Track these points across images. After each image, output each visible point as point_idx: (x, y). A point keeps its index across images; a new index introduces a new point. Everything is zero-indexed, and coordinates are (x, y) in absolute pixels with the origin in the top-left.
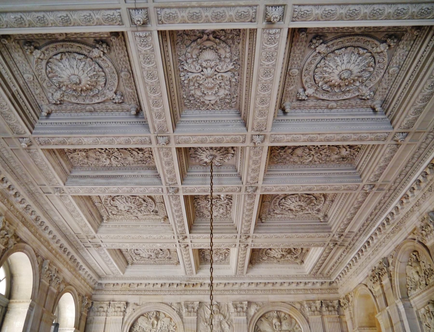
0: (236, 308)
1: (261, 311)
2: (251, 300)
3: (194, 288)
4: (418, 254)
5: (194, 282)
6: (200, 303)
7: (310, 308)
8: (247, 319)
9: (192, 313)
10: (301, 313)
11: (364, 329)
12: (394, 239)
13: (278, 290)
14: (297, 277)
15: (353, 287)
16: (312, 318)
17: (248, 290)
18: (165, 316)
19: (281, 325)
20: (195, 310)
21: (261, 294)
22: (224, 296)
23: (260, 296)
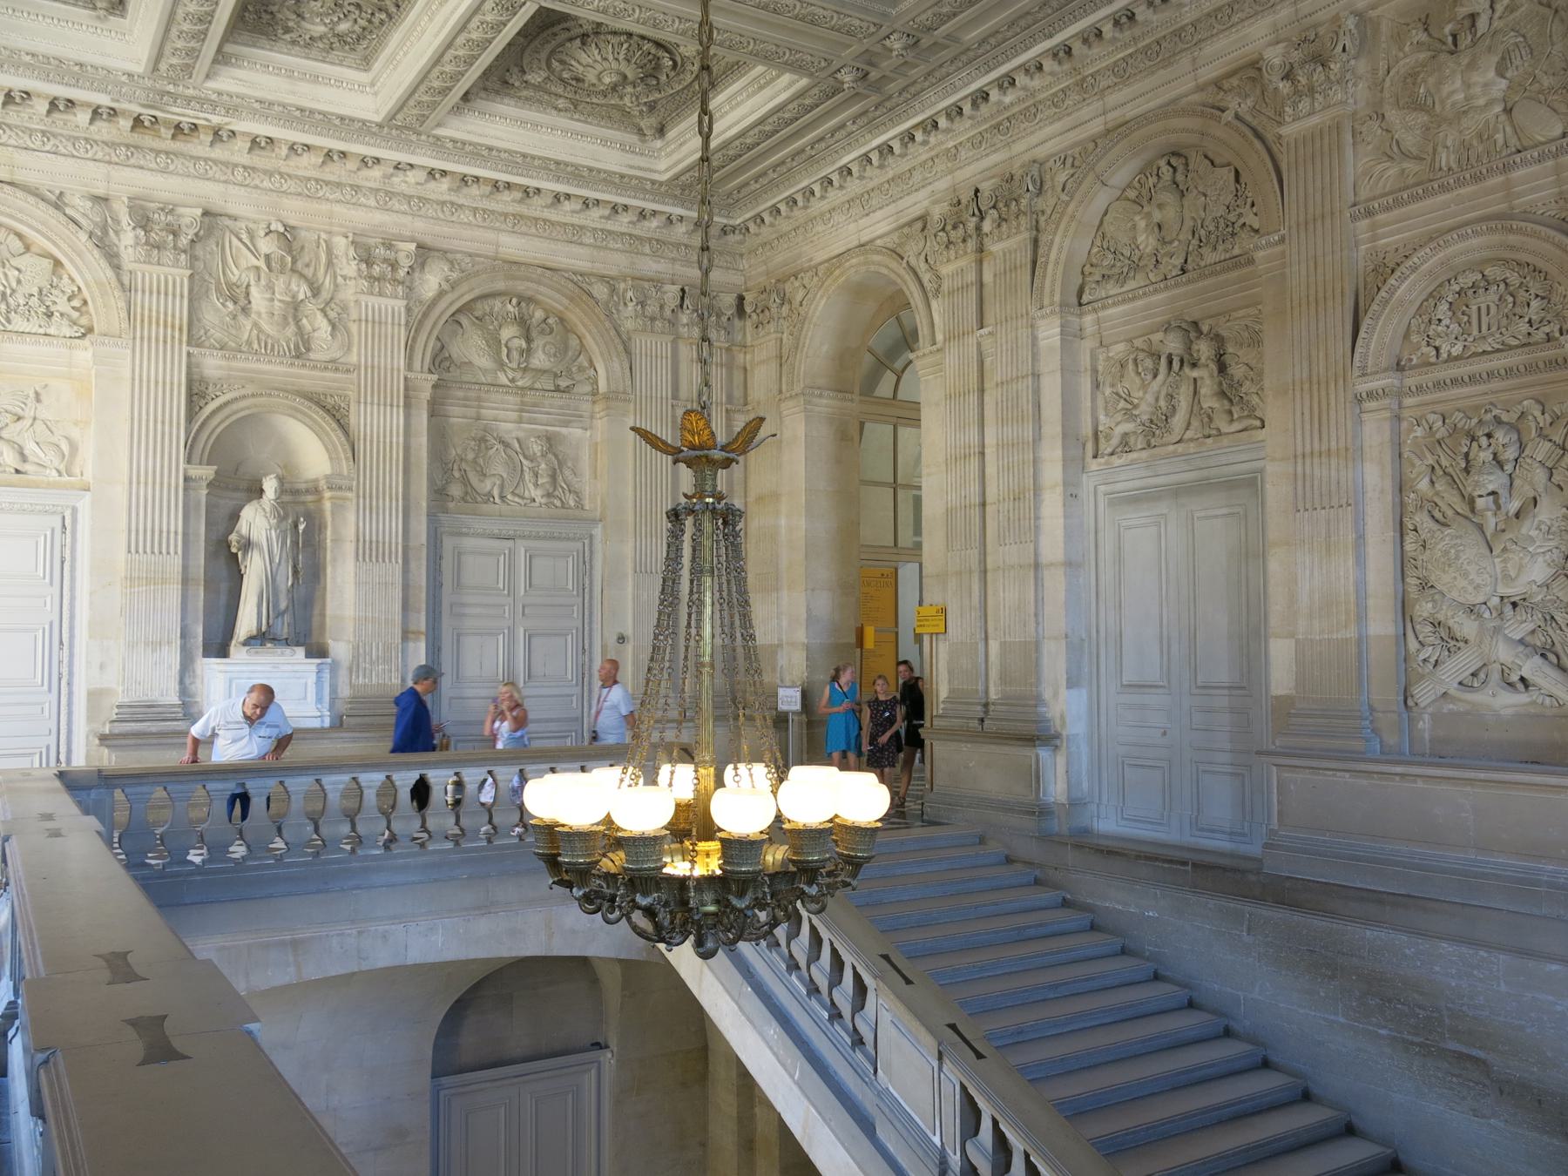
0: (368, 261)
1: (464, 287)
2: (428, 240)
3: (177, 145)
4: (1187, 164)
5: (186, 116)
6: (206, 213)
7: (643, 304)
8: (408, 310)
9: (168, 255)
10: (609, 316)
11: (821, 396)
12: (1113, 98)
13: (536, 219)
14: (619, 181)
15: (820, 256)
16: (641, 343)
17: (419, 198)
18: (27, 248)
19: (529, 350)
20: (184, 241)
21: (469, 224)
22: (314, 206)
23: (467, 233)
